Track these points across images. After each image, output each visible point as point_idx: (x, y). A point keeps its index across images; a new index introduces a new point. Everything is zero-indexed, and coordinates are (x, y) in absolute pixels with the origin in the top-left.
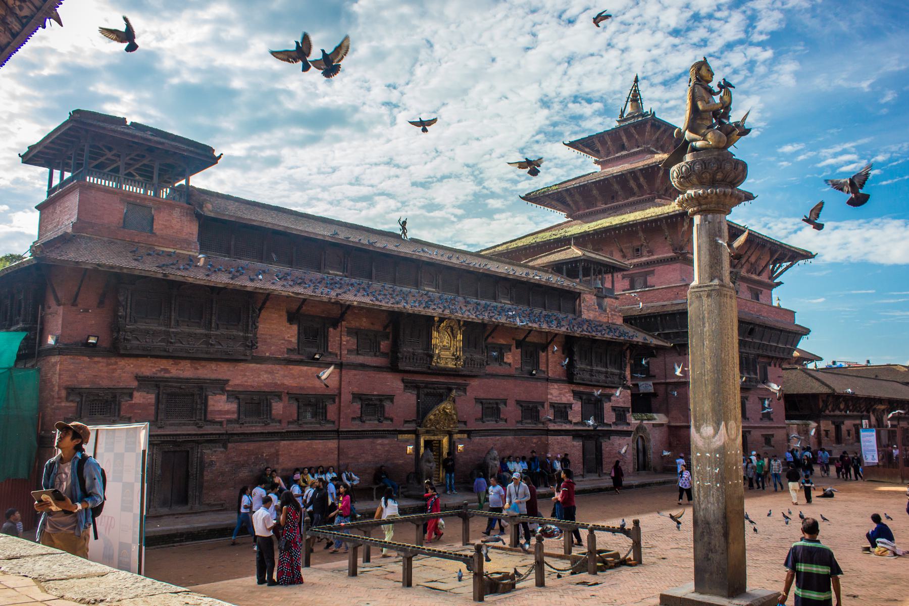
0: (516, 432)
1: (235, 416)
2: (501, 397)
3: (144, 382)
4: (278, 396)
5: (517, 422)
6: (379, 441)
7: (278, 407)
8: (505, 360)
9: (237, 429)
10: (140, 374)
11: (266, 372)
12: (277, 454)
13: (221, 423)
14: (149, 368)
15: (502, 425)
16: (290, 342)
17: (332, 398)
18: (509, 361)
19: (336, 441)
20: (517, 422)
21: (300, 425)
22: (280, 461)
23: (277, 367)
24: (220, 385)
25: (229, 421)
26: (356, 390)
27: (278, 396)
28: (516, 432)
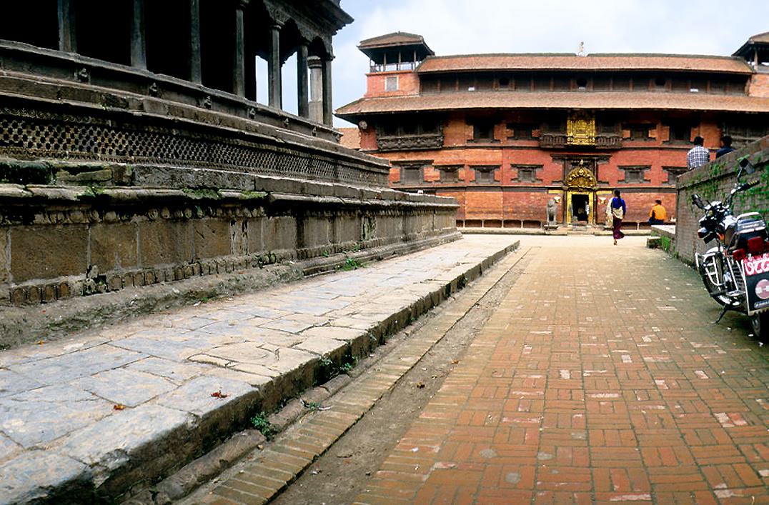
0: (659, 190)
1: (439, 179)
2: (645, 164)
3: (394, 163)
4: (462, 166)
5: (663, 183)
6: (533, 193)
7: (462, 172)
8: (650, 136)
9: (440, 185)
10: (392, 160)
11: (454, 154)
12: (464, 199)
13: (431, 182)
14: (395, 158)
15: (646, 185)
16: (469, 136)
17: (498, 167)
18: (653, 137)
19: (502, 192)
20: (663, 183)
21: (477, 183)
22: (466, 202)
23: (461, 151)
24: (429, 163)
25: (436, 181)
26: (514, 163)
27: (462, 166)
28: (659, 190)
